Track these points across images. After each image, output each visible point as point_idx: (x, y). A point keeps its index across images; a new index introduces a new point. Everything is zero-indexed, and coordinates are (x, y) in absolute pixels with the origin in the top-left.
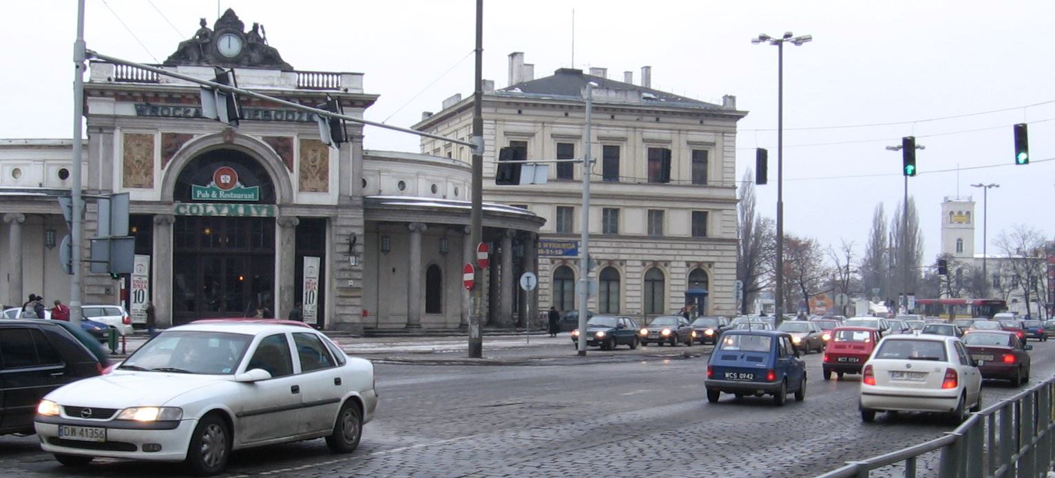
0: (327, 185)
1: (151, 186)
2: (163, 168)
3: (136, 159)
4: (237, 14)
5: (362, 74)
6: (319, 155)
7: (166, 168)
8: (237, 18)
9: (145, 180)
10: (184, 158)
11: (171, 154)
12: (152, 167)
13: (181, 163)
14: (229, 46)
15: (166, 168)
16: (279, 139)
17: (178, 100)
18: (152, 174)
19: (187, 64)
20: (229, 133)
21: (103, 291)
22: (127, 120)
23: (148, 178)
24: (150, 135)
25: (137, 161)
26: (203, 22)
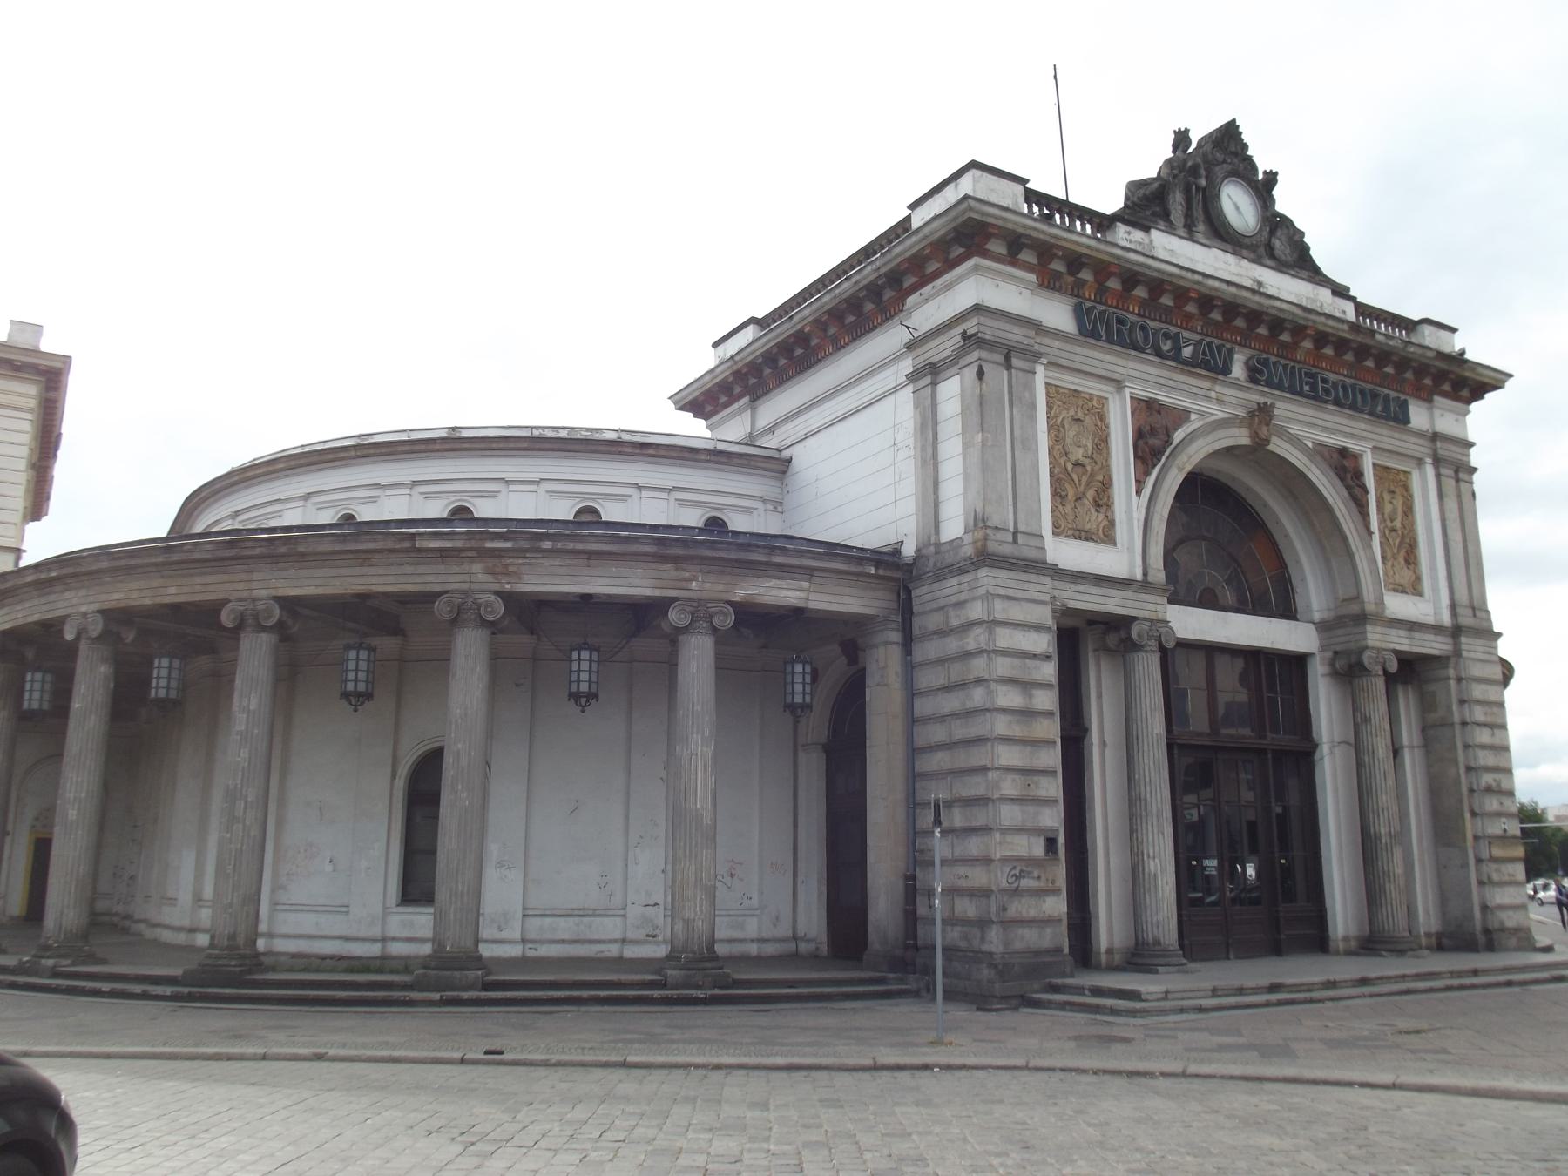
0: (1418, 579)
1: (1107, 537)
2: (1138, 492)
3: (1073, 458)
4: (1246, 137)
5: (1454, 330)
6: (1399, 502)
7: (1147, 492)
8: (1245, 147)
9: (1094, 520)
10: (1181, 469)
11: (1156, 454)
12: (1106, 485)
13: (1174, 480)
14: (1236, 204)
15: (1147, 492)
16: (1343, 452)
17: (1166, 315)
18: (1109, 506)
19: (1170, 230)
20: (1262, 413)
21: (1039, 850)
22: (1057, 344)
23: (1101, 516)
24: (1100, 398)
25: (1077, 464)
26: (1181, 138)
